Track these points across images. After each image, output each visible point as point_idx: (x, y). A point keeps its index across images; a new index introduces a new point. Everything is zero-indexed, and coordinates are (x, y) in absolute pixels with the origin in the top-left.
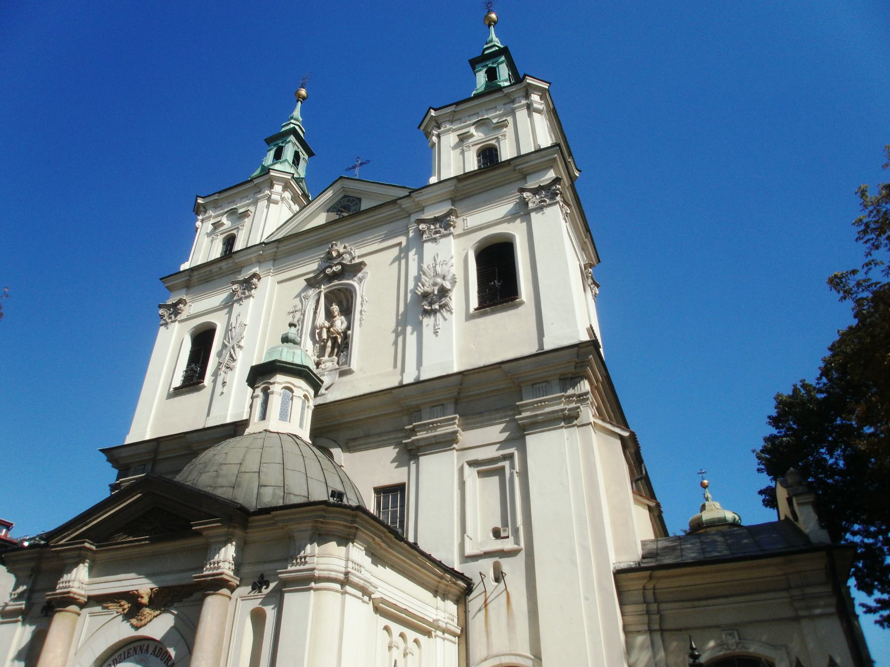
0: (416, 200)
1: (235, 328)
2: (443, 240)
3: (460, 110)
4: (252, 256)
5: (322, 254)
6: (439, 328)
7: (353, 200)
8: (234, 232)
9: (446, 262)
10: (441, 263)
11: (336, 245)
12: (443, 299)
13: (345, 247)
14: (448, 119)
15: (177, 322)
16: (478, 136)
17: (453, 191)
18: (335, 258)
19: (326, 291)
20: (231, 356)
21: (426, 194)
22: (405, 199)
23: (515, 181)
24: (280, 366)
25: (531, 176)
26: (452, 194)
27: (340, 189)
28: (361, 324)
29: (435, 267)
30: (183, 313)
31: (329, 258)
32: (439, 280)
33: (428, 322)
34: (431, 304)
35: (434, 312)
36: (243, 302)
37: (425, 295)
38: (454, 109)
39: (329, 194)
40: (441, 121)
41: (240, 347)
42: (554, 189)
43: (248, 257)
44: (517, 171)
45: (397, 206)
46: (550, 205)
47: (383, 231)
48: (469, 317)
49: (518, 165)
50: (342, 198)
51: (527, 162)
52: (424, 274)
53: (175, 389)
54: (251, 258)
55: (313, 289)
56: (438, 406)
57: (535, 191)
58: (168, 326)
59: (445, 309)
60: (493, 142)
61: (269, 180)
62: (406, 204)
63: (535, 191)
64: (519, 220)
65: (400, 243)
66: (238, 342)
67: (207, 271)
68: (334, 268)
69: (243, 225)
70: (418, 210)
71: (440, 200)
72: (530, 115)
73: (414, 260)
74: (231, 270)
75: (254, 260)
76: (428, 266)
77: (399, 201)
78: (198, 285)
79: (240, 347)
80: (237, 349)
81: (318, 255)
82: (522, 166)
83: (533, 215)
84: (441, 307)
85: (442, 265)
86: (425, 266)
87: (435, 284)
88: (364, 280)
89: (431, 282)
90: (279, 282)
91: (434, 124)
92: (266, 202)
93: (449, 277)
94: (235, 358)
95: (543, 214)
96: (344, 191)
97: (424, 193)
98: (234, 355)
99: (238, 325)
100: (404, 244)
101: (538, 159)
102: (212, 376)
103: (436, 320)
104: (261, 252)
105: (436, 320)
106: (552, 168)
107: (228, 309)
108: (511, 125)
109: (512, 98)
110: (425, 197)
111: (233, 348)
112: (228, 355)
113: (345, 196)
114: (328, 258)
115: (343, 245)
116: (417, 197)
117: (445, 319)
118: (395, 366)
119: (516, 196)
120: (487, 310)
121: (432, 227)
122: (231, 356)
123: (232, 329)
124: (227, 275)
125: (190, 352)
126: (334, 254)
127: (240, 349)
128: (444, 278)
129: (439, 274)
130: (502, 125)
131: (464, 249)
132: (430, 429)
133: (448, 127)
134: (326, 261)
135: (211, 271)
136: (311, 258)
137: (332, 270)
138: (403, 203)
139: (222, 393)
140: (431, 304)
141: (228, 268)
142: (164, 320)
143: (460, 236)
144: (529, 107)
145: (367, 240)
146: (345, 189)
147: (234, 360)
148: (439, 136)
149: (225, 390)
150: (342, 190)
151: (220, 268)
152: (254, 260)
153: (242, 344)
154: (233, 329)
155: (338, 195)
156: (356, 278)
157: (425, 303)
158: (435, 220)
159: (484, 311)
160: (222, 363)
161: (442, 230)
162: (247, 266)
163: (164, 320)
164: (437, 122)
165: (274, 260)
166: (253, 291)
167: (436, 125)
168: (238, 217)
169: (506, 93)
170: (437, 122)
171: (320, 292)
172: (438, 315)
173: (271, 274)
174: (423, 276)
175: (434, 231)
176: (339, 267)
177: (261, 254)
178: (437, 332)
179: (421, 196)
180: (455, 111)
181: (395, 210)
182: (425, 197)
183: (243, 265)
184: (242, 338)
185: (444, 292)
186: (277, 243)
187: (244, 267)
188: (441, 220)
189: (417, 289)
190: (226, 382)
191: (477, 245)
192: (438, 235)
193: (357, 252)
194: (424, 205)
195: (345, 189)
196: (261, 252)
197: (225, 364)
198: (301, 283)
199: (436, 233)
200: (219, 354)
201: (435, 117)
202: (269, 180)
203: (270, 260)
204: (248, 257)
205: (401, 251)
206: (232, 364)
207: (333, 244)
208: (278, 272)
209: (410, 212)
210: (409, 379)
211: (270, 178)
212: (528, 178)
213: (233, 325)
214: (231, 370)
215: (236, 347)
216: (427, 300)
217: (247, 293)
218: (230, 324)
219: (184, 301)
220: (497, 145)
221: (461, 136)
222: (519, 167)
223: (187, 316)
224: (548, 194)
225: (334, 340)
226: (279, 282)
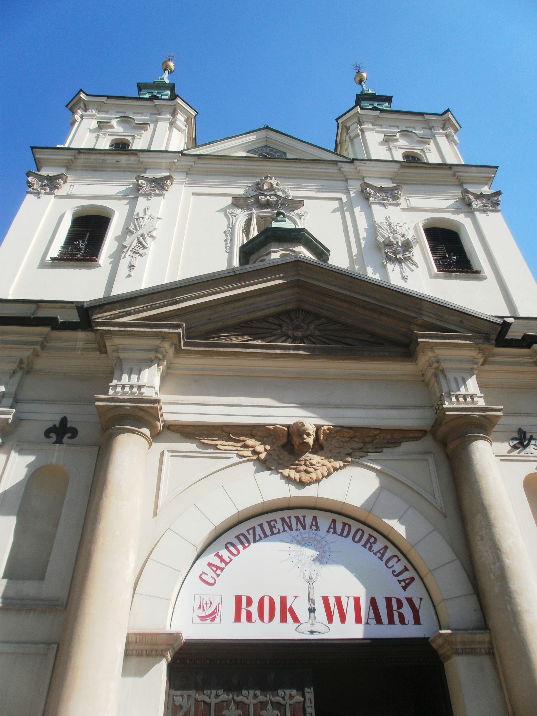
1: (143, 218)
2: (391, 207)
3: (382, 118)
4: (163, 161)
5: (250, 183)
6: (407, 276)
7: (277, 152)
8: (129, 138)
9: (400, 225)
10: (395, 224)
11: (271, 178)
12: (406, 253)
13: (277, 184)
14: (371, 120)
15: (53, 196)
17: (396, 172)
18: (265, 191)
19: (258, 215)
20: (139, 242)
21: (368, 166)
22: (347, 164)
23: (451, 185)
24: (307, 238)
26: (393, 175)
27: (263, 138)
30: (61, 190)
31: (258, 187)
35: (400, 261)
36: (151, 197)
37: (389, 244)
38: (378, 114)
39: (252, 137)
40: (366, 120)
41: (151, 236)
42: (496, 200)
43: (160, 161)
44: (456, 177)
45: (336, 168)
46: (492, 211)
47: (322, 183)
49: (458, 172)
50: (263, 147)
51: (467, 172)
53: (53, 259)
54: (162, 162)
55: (240, 210)
58: (40, 196)
59: (409, 262)
61: (174, 107)
65: (341, 199)
66: (150, 232)
67: (98, 159)
68: (268, 197)
69: (141, 136)
70: (356, 178)
71: (382, 176)
74: (130, 168)
75: (164, 165)
77: (338, 163)
78: (82, 170)
79: (151, 236)
80: (148, 239)
81: (247, 183)
82: (462, 174)
83: (477, 214)
85: (396, 226)
88: (303, 217)
90: (194, 194)
91: (356, 120)
92: (167, 125)
94: (147, 246)
95: (487, 216)
96: (266, 140)
97: (367, 164)
98: (144, 242)
99: (147, 216)
101: (478, 173)
102: (111, 257)
104: (176, 160)
106: (486, 185)
107: (128, 201)
109: (431, 125)
110: (368, 169)
111: (142, 235)
112: (136, 242)
113: (266, 146)
114: (256, 188)
115: (276, 183)
116: (360, 166)
117: (412, 271)
119: (457, 196)
120: (452, 274)
122: (139, 242)
123: (139, 218)
124: (124, 171)
125: (69, 230)
126: (266, 187)
127: (152, 239)
129: (397, 232)
133: (371, 126)
134: (254, 190)
135: (104, 161)
136: (236, 183)
137: (267, 199)
138: (343, 166)
139: (129, 276)
140: (395, 253)
141: (127, 164)
142: (33, 189)
143: (404, 209)
144: (447, 136)
145: (302, 186)
146: (268, 140)
147: (144, 247)
148: (362, 131)
149: (133, 273)
150: (265, 139)
151: (118, 162)
152: (164, 165)
153: (154, 234)
154: (141, 219)
155: (259, 143)
156: (293, 213)
158: (381, 189)
159: (449, 274)
160: (126, 247)
161: (391, 200)
162: (153, 168)
163: (33, 189)
165: (187, 174)
166: (164, 192)
167: (358, 121)
168: (134, 127)
169: (427, 119)
171: (251, 214)
173: (184, 183)
175: (381, 198)
176: (274, 198)
177: (174, 162)
178: (407, 279)
179: (366, 166)
180: (378, 117)
181: (333, 170)
182: (368, 169)
183: (149, 167)
184: (155, 229)
185: (407, 246)
186: (195, 158)
187: (149, 169)
188: (387, 192)
189: (377, 237)
190: (135, 266)
191: (425, 222)
194: (364, 175)
195: (268, 140)
196: (176, 160)
197: (131, 249)
198: (228, 201)
200: (120, 239)
201: (360, 114)
202: (173, 107)
203: (183, 172)
204: (160, 161)
206: (141, 251)
207: (267, 177)
208: (193, 185)
209: (347, 177)
211: (175, 105)
213: (141, 215)
214: (141, 255)
215: (146, 236)
216: (390, 249)
217: (157, 192)
218: (135, 213)
219: (65, 178)
221: (388, 137)
222: (460, 174)
223: (67, 194)
224: (488, 202)
226: (194, 194)
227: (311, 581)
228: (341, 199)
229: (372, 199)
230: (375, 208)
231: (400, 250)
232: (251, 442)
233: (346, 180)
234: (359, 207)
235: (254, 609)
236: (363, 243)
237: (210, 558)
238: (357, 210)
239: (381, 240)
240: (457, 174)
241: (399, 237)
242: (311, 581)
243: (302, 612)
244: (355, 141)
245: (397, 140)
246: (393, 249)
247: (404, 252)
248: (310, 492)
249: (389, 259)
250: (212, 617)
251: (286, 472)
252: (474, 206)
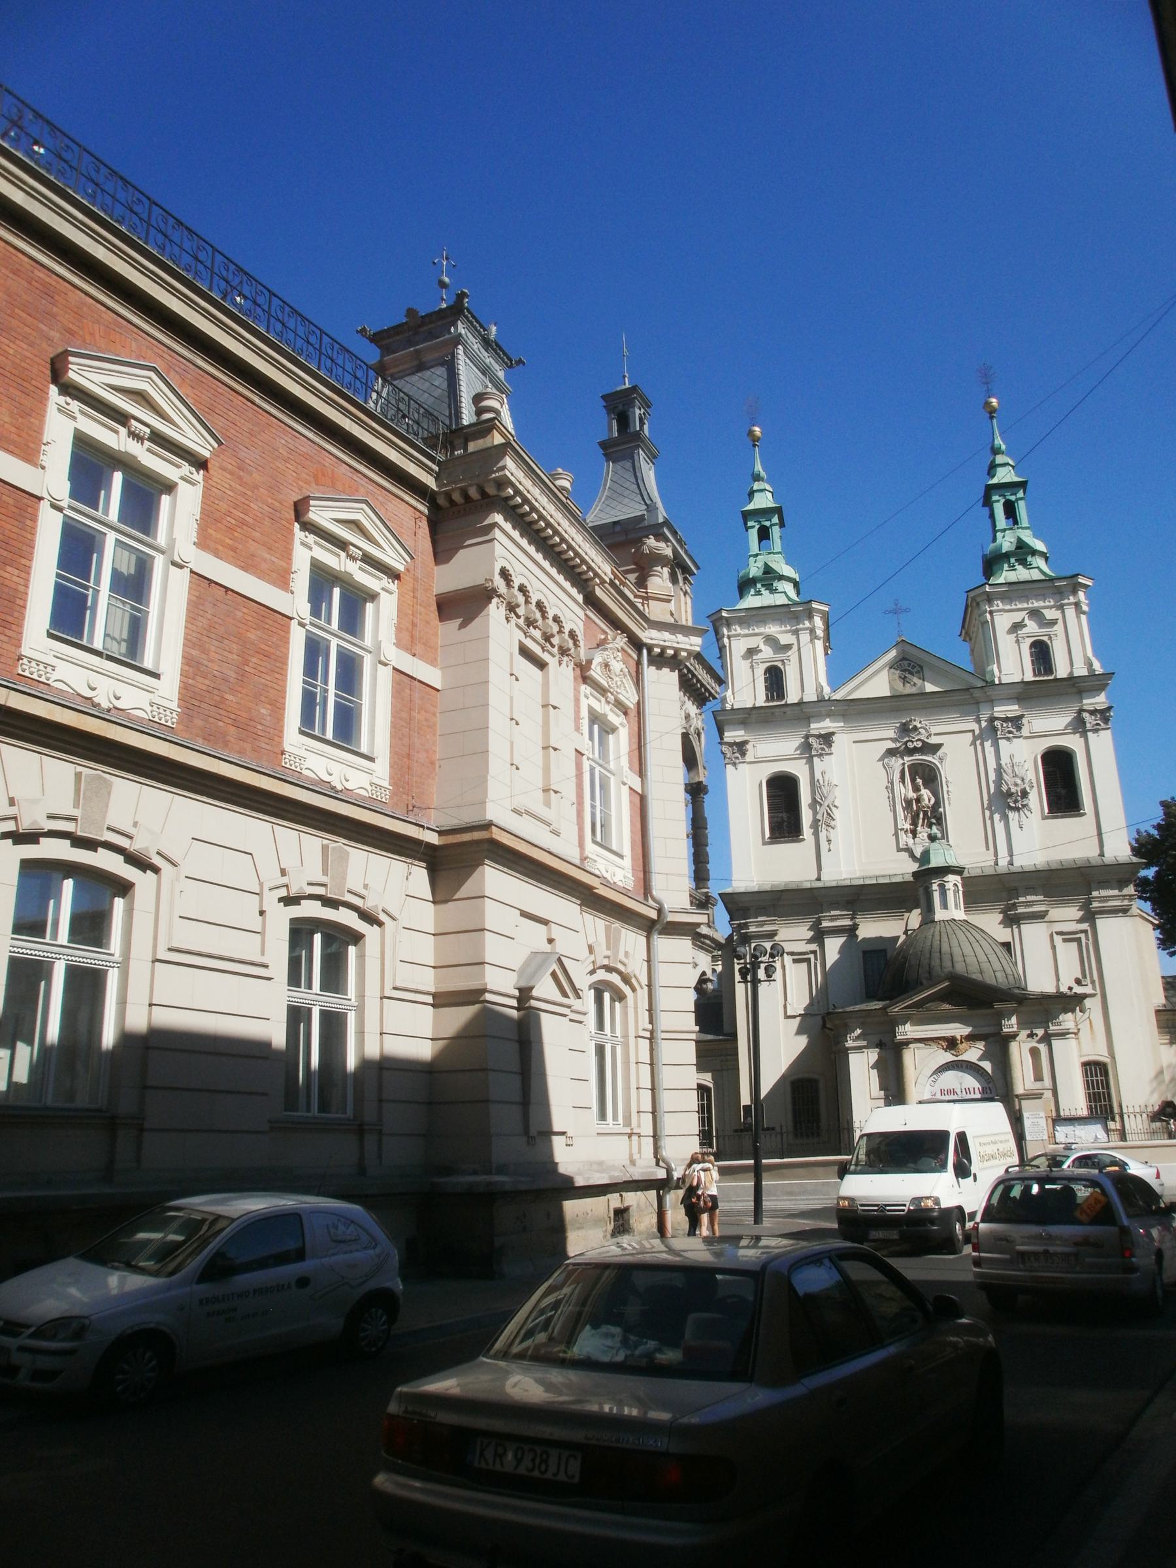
0: (988, 694)
2: (1015, 740)
16: (1032, 627)
25: (1088, 693)
28: (949, 803)
29: (1013, 767)
32: (1019, 782)
33: (1012, 815)
34: (1016, 802)
35: (1017, 809)
37: (1010, 794)
48: (1044, 818)
52: (1005, 771)
56: (1031, 890)
57: (1093, 712)
60: (1045, 639)
62: (977, 693)
63: (1093, 712)
64: (1078, 735)
65: (973, 731)
72: (1078, 617)
73: (990, 753)
76: (1006, 764)
84: (1024, 806)
86: (1003, 763)
87: (1016, 785)
88: (944, 761)
89: (1013, 781)
91: (986, 597)
93: (1026, 781)
100: (977, 732)
103: (1019, 815)
105: (1019, 815)
108: (1060, 622)
110: (996, 693)
118: (988, 848)
121: (1005, 725)
128: (1023, 780)
130: (1053, 623)
131: (1032, 753)
132: (1029, 906)
133: (1001, 606)
140: (1016, 802)
144: (1077, 605)
148: (991, 613)
157: (1009, 800)
158: (1007, 719)
161: (1014, 730)
164: (988, 596)
170: (988, 596)
172: (1021, 811)
174: (1004, 774)
185: (1025, 794)
192: (1011, 735)
193: (934, 730)
199: (1010, 732)
205: (975, 739)
210: (1003, 862)
212: (1084, 694)
220: (1050, 644)
225: (925, 813)
227: (961, 1084)
228: (973, 731)
229: (999, 733)
230: (1002, 743)
231: (1019, 798)
232: (940, 1042)
233: (978, 703)
234: (990, 741)
235: (946, 1092)
236: (992, 791)
237: (932, 1078)
238: (988, 744)
239: (1004, 788)
240: (1077, 685)
241: (1019, 782)
242: (961, 1084)
243: (959, 1093)
244: (985, 626)
245: (1025, 626)
246: (1014, 798)
247: (1022, 799)
248: (960, 1058)
249: (1011, 808)
250: (935, 1095)
251: (952, 1052)
252: (1088, 726)
